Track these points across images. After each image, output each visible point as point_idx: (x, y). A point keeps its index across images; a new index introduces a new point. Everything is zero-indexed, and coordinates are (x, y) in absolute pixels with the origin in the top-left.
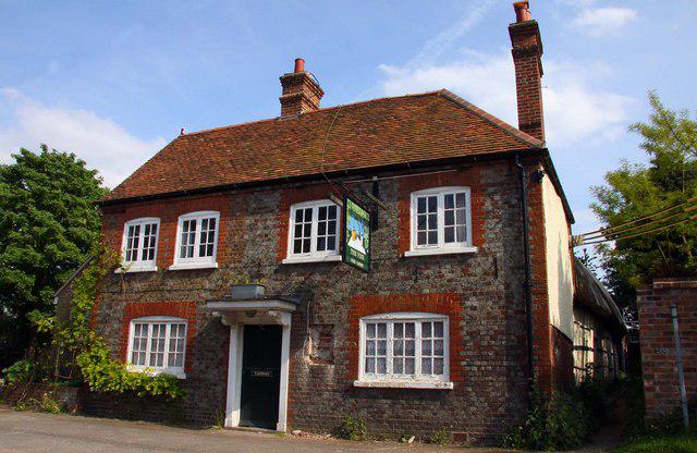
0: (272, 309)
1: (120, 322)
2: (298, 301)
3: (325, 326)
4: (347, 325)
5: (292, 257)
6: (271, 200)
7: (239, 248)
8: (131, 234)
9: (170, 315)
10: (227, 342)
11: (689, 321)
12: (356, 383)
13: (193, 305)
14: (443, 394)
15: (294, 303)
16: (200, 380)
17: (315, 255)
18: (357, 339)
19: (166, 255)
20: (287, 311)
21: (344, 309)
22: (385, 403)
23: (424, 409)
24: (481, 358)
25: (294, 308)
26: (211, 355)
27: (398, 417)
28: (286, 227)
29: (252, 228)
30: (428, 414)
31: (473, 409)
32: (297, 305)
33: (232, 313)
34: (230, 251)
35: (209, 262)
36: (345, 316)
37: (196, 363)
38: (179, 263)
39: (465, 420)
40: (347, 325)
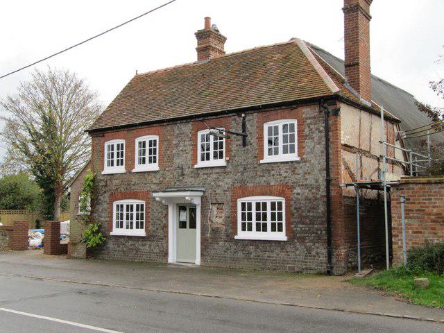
0: (187, 196)
1: (107, 204)
2: (203, 189)
3: (219, 204)
4: (231, 204)
5: (201, 164)
6: (187, 128)
7: (171, 158)
8: (118, 210)
9: (136, 198)
10: (167, 215)
11: (419, 203)
12: (236, 237)
13: (148, 192)
14: (282, 243)
15: (201, 191)
16: (154, 236)
17: (213, 162)
18: (236, 212)
19: (130, 165)
20: (197, 196)
21: (229, 194)
22: (252, 248)
23: (272, 251)
24: (303, 223)
25: (201, 194)
26: (159, 222)
27: (259, 256)
28: (196, 145)
29: (177, 146)
30: (274, 255)
31: (298, 252)
32: (204, 192)
33: (170, 199)
34: (166, 160)
35: (154, 167)
36: (229, 198)
37: (151, 227)
38: (139, 168)
39: (294, 258)
40: (231, 204)
